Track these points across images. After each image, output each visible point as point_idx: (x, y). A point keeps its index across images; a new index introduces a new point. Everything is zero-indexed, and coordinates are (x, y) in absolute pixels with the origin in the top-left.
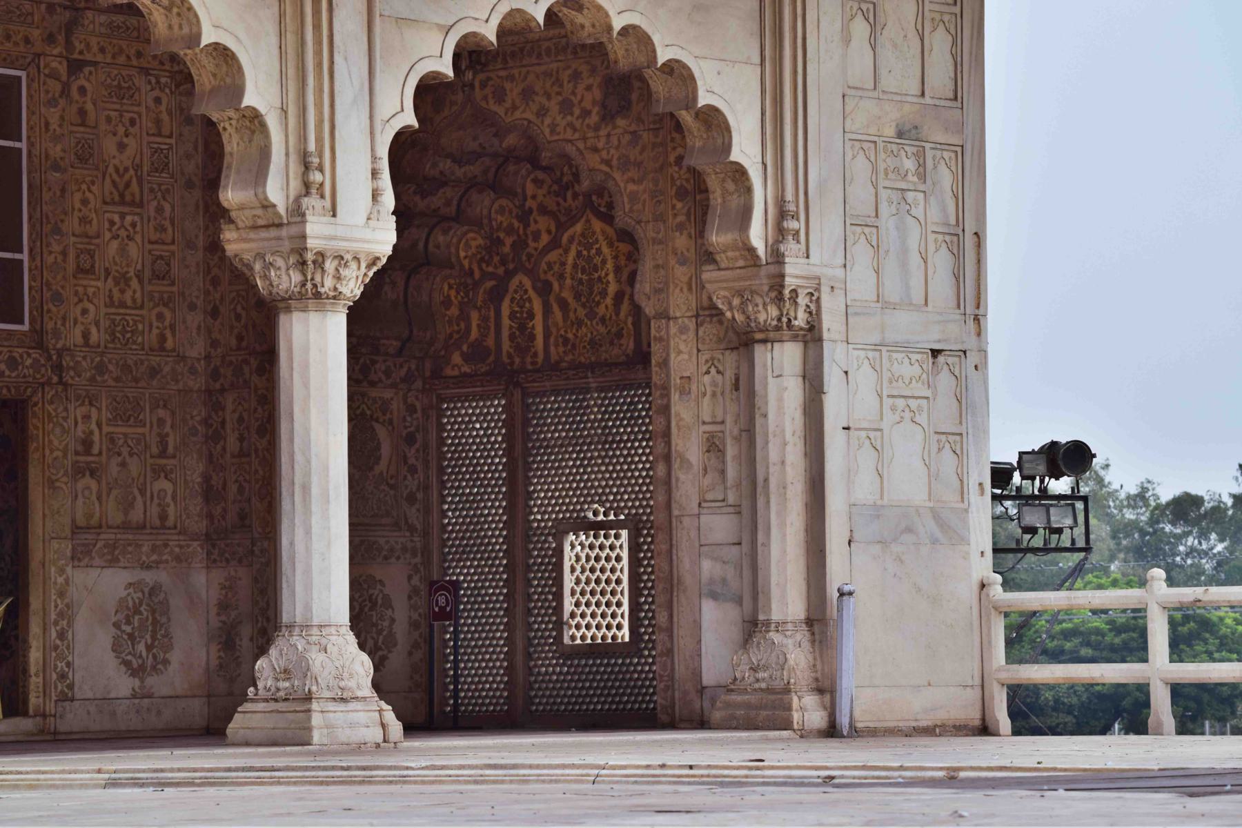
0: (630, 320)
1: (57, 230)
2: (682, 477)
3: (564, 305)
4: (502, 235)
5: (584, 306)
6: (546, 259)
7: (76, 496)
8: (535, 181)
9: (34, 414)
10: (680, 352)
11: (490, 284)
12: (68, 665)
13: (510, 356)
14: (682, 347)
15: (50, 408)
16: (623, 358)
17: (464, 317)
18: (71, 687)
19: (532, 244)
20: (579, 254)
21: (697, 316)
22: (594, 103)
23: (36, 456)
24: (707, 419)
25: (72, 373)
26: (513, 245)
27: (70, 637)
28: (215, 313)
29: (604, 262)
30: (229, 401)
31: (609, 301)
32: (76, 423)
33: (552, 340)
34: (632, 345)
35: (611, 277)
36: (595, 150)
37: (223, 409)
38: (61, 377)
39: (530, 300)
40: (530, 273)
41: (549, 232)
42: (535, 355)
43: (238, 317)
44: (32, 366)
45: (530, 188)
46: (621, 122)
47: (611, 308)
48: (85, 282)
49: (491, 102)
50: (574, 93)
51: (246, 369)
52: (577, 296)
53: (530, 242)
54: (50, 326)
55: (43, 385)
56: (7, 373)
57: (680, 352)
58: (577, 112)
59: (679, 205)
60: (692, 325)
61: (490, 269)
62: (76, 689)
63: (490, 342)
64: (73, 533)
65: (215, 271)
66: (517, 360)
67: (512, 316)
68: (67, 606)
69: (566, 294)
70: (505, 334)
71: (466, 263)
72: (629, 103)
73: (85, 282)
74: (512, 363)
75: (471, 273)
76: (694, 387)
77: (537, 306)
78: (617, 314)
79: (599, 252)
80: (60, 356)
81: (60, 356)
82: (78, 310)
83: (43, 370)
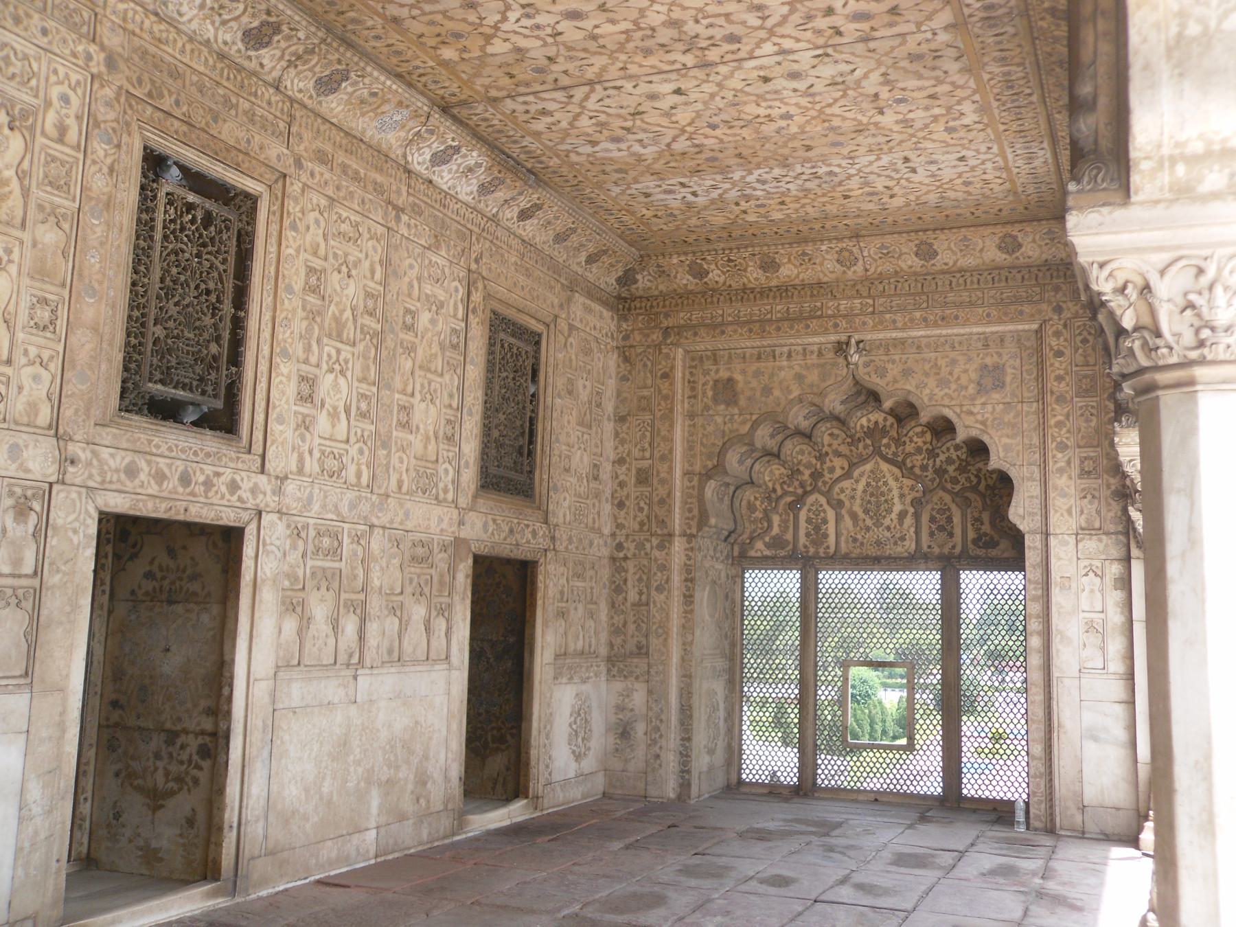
0: (913, 529)
1: (558, 440)
2: (1060, 647)
3: (854, 516)
4: (802, 468)
5: (871, 518)
6: (840, 485)
8: (831, 435)
10: (1060, 559)
11: (789, 499)
13: (805, 547)
14: (1062, 555)
16: (906, 554)
17: (767, 517)
19: (827, 476)
20: (868, 484)
21: (1077, 534)
22: (970, 380)
24: (1086, 609)
26: (812, 475)
28: (621, 505)
29: (890, 490)
30: (630, 566)
31: (894, 516)
33: (843, 539)
34: (913, 546)
35: (896, 500)
36: (971, 413)
37: (626, 571)
39: (824, 511)
40: (827, 494)
41: (843, 468)
42: (828, 547)
43: (641, 510)
45: (827, 439)
46: (996, 396)
47: (896, 521)
49: (874, 376)
50: (951, 374)
51: (648, 546)
52: (866, 512)
53: (826, 473)
54: (551, 507)
57: (1060, 559)
58: (953, 386)
59: (1060, 455)
60: (1072, 540)
61: (791, 489)
63: (789, 536)
65: (621, 477)
66: (812, 550)
67: (809, 521)
69: (857, 508)
70: (802, 532)
71: (770, 485)
72: (1004, 383)
74: (807, 552)
75: (774, 490)
76: (1074, 585)
77: (831, 514)
78: (901, 524)
79: (885, 484)
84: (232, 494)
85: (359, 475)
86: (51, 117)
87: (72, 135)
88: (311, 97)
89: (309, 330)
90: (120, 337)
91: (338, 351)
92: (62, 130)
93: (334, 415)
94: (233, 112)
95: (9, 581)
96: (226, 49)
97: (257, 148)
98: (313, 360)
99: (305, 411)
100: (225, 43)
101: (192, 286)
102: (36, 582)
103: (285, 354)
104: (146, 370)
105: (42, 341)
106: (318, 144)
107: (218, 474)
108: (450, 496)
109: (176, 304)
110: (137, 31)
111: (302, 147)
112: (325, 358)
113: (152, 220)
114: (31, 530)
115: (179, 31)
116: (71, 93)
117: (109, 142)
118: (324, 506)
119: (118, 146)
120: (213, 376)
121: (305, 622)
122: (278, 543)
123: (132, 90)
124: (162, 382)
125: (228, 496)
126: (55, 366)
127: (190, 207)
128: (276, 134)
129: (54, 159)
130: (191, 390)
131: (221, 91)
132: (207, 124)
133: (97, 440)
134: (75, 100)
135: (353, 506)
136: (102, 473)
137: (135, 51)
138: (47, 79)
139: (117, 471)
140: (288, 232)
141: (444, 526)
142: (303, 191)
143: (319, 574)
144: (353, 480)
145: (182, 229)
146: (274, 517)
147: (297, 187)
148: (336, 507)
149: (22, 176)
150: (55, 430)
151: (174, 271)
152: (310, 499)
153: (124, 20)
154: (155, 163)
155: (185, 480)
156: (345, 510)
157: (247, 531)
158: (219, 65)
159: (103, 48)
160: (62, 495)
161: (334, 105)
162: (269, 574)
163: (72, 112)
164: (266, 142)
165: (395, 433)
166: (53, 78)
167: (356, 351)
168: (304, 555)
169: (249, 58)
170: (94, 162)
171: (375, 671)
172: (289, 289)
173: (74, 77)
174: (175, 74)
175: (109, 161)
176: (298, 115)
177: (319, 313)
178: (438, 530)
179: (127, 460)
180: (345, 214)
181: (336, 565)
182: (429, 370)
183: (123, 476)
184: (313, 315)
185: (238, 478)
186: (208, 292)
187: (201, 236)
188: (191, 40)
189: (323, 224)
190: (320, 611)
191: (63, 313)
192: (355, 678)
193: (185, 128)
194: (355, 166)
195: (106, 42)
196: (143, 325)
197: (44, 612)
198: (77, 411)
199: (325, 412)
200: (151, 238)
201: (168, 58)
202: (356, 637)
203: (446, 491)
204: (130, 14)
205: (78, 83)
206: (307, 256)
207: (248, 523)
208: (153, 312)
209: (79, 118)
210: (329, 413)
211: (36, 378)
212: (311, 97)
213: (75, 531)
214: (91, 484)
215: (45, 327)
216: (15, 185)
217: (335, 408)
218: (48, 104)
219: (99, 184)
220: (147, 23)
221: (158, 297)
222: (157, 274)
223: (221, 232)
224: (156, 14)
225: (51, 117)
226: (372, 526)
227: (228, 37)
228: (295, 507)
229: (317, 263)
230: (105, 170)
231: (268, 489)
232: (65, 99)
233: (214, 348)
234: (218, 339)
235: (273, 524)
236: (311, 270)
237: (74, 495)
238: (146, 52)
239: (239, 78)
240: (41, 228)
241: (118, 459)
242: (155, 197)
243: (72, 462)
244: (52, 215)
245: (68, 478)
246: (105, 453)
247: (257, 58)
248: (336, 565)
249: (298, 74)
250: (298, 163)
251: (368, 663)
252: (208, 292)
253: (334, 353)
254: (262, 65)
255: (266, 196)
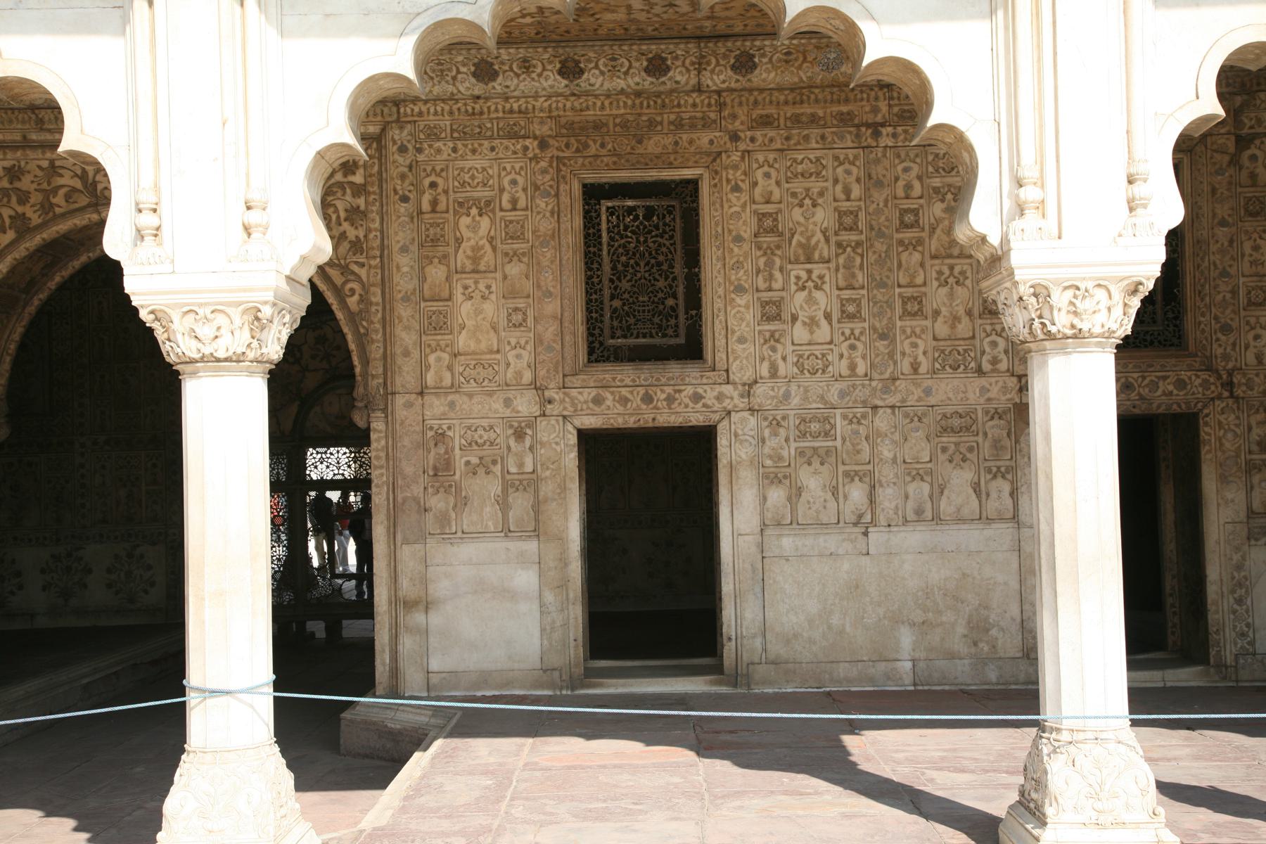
7: (1252, 488)
9: (1206, 424)
12: (1248, 625)
15: (1222, 418)
18: (1252, 643)
23: (1209, 456)
25: (1244, 388)
27: (1249, 602)
32: (1250, 429)
38: (1231, 393)
44: (1201, 385)
48: (1257, 313)
55: (1213, 399)
56: (1175, 392)
62: (1257, 645)
64: (1248, 517)
68: (1245, 578)
73: (1257, 313)
80: (1230, 374)
81: (1230, 374)
82: (1250, 336)
83: (1213, 388)
84: (696, 403)
85: (853, 367)
86: (506, 197)
87: (522, 203)
88: (737, 81)
89: (769, 264)
90: (580, 316)
91: (809, 272)
92: (514, 202)
93: (812, 323)
94: (659, 128)
95: (516, 477)
96: (640, 87)
97: (686, 144)
98: (776, 286)
99: (772, 327)
100: (638, 84)
101: (642, 264)
102: (534, 476)
103: (740, 289)
104: (607, 332)
105: (518, 334)
106: (759, 112)
107: (680, 391)
108: (1003, 366)
109: (630, 281)
110: (561, 113)
111: (737, 123)
112: (793, 280)
113: (600, 230)
114: (528, 446)
115: (596, 96)
116: (518, 177)
117: (549, 195)
118: (806, 399)
119: (557, 195)
120: (673, 322)
121: (796, 493)
122: (752, 433)
123: (561, 154)
124: (625, 337)
125: (691, 405)
126: (530, 347)
127: (631, 210)
128: (707, 124)
129: (511, 222)
130: (652, 336)
131: (645, 118)
132: (632, 148)
133: (569, 385)
134: (521, 180)
135: (842, 395)
136: (573, 404)
137: (563, 127)
138: (499, 176)
139: (586, 402)
140: (730, 196)
141: (992, 394)
142: (743, 158)
143: (809, 453)
144: (845, 372)
145: (626, 229)
146: (746, 414)
147: (736, 157)
148: (822, 397)
149: (491, 240)
150: (537, 387)
151: (623, 259)
152: (787, 396)
153: (550, 111)
154: (593, 193)
155: (648, 399)
156: (833, 397)
157: (719, 427)
158: (637, 102)
159: (535, 138)
160: (544, 423)
161: (764, 75)
162: (744, 456)
163: (519, 188)
164: (694, 136)
165: (899, 324)
166: (503, 173)
167: (832, 265)
168: (787, 440)
169: (664, 83)
170: (539, 213)
171: (892, 529)
172: (738, 239)
173: (517, 166)
174: (598, 126)
175: (550, 207)
176: (728, 100)
177: (778, 247)
178: (982, 401)
179: (593, 394)
180: (800, 157)
181: (830, 444)
182: (950, 256)
183: (591, 405)
184: (769, 252)
185: (700, 391)
186: (659, 264)
187: (645, 227)
188: (608, 96)
189: (773, 173)
190: (813, 482)
191: (530, 313)
192: (866, 534)
193: (615, 159)
194: (809, 111)
195: (538, 133)
196: (602, 303)
197: (542, 494)
198: (548, 371)
199: (798, 324)
200: (600, 243)
201: (591, 119)
202: (866, 501)
203: (995, 361)
204: (554, 105)
205: (521, 168)
206: (754, 207)
207: (719, 422)
208: (607, 292)
209: (525, 190)
210: (804, 323)
211: (518, 357)
212: (737, 81)
213: (557, 443)
214: (565, 413)
215: (521, 325)
216: (488, 247)
217: (812, 319)
218: (502, 190)
219: (547, 225)
220: (569, 105)
221: (611, 281)
222: (607, 267)
223: (664, 216)
224: (574, 95)
225: (506, 197)
226: (875, 408)
227: (637, 79)
228: (768, 404)
229: (770, 208)
230: (548, 214)
231: (735, 394)
232: (514, 182)
233: (670, 302)
234: (675, 296)
235: (743, 420)
236: (762, 217)
237: (553, 422)
238: (573, 123)
239: (659, 101)
240: (508, 268)
241: (585, 395)
242: (599, 215)
243: (550, 402)
244: (510, 257)
245: (547, 412)
246: (574, 392)
247: (670, 79)
248: (830, 444)
249: (712, 72)
250: (735, 137)
251: (882, 520)
252: (659, 264)
253: (804, 275)
254: (677, 82)
255: (706, 175)
